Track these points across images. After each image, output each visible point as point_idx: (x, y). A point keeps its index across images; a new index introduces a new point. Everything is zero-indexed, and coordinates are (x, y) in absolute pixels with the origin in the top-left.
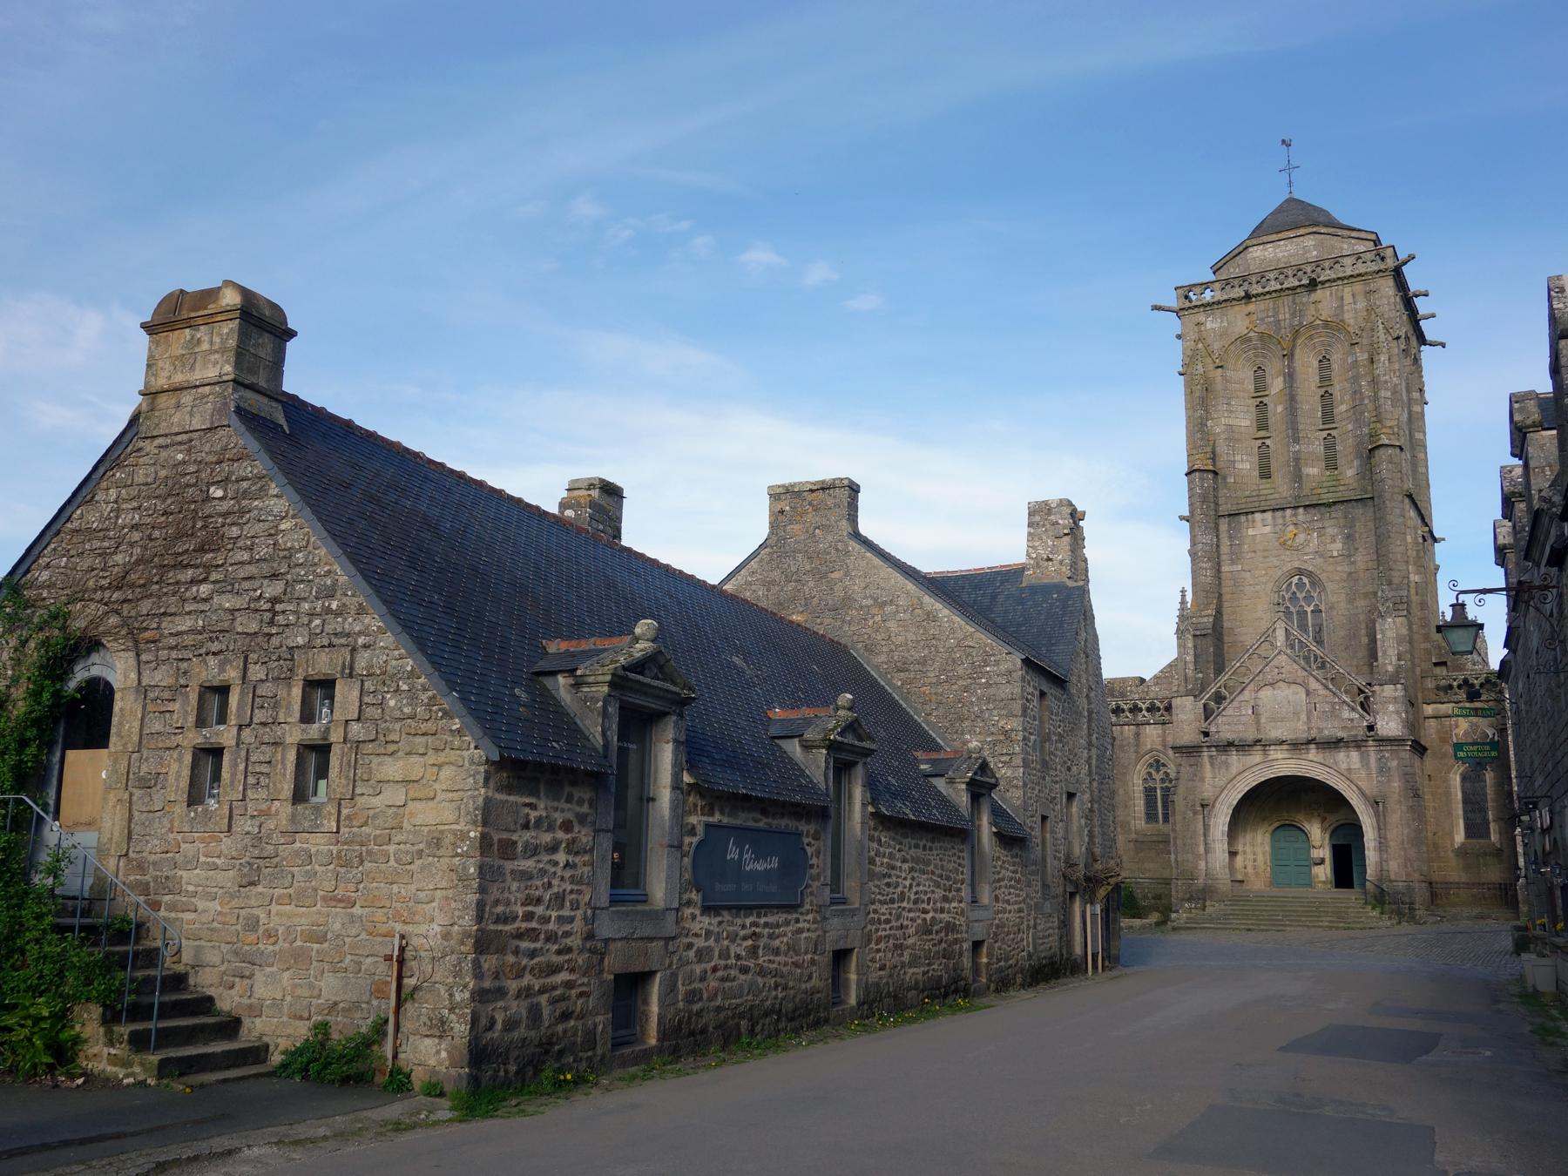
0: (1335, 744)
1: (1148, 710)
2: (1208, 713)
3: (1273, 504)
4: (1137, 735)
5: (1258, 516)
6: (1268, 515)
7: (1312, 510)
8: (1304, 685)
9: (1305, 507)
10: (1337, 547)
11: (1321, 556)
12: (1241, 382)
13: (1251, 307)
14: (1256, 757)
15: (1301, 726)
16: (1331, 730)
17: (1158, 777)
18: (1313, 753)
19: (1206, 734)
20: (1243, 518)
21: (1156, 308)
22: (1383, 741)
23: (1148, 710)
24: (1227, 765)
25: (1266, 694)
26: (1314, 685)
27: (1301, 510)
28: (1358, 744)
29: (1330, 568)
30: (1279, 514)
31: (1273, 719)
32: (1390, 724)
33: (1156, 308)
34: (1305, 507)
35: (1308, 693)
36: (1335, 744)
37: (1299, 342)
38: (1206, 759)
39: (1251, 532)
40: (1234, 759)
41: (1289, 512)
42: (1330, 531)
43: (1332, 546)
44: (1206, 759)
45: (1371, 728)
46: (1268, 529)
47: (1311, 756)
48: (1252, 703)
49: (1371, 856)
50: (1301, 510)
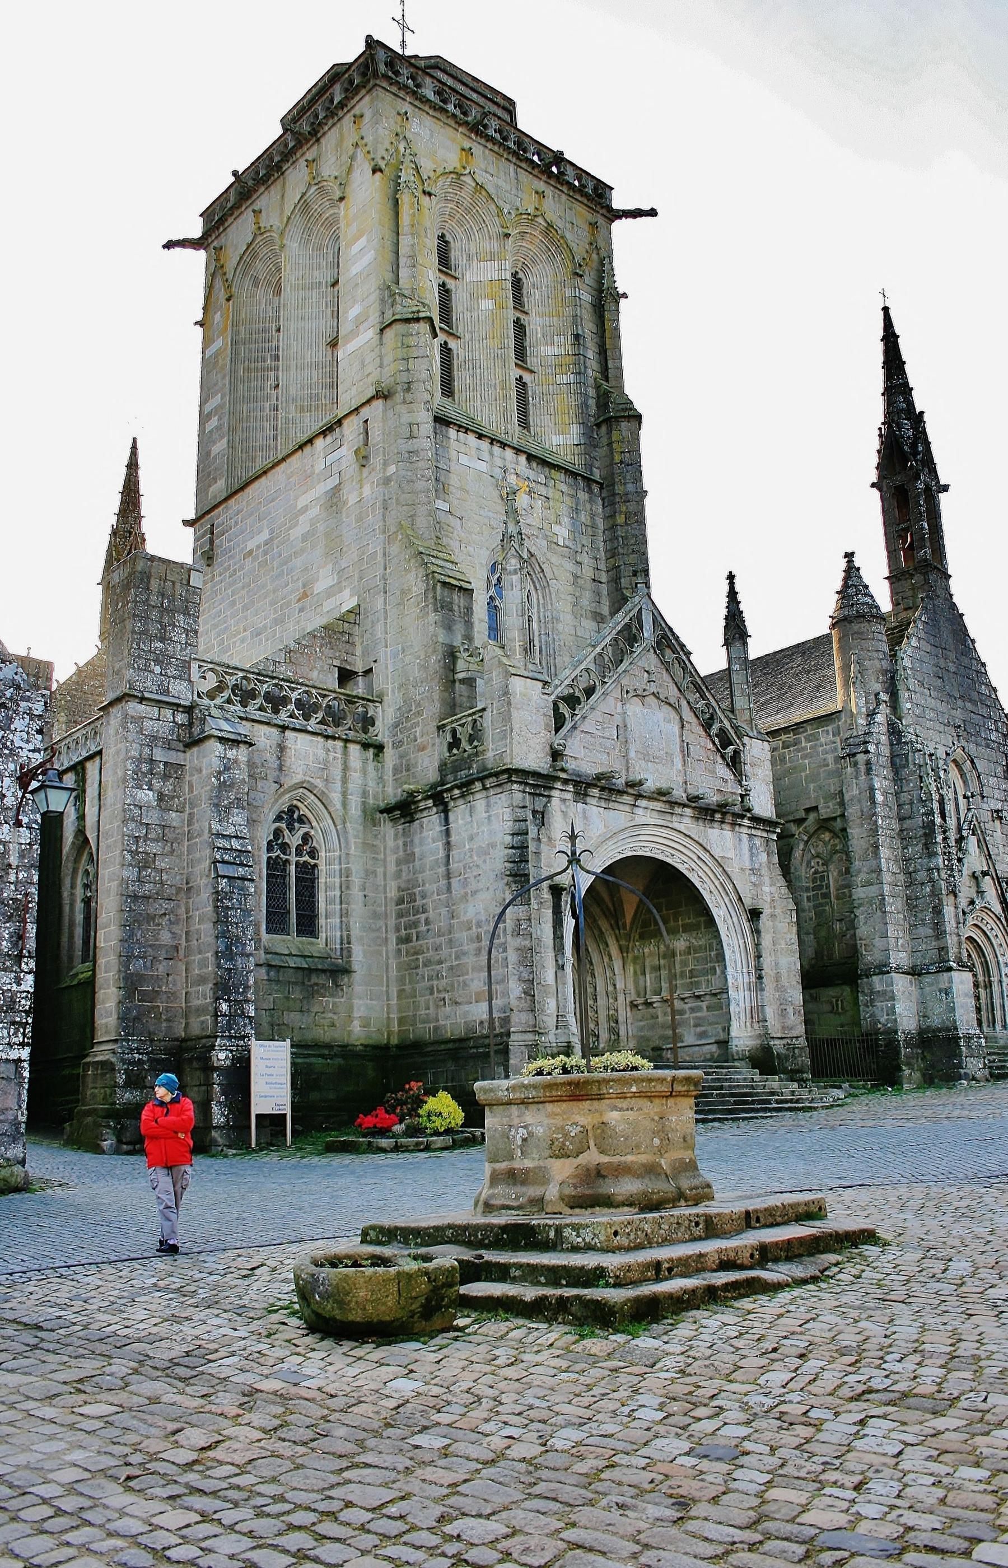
1: (299, 704)
4: (282, 748)
8: (677, 710)
17: (294, 840)
18: (686, 822)
22: (756, 820)
23: (299, 704)
25: (634, 708)
30: (497, 449)
31: (646, 757)
38: (555, 802)
43: (556, 528)
46: (482, 466)
47: (681, 827)
48: (618, 720)
49: (739, 999)
50: (523, 458)
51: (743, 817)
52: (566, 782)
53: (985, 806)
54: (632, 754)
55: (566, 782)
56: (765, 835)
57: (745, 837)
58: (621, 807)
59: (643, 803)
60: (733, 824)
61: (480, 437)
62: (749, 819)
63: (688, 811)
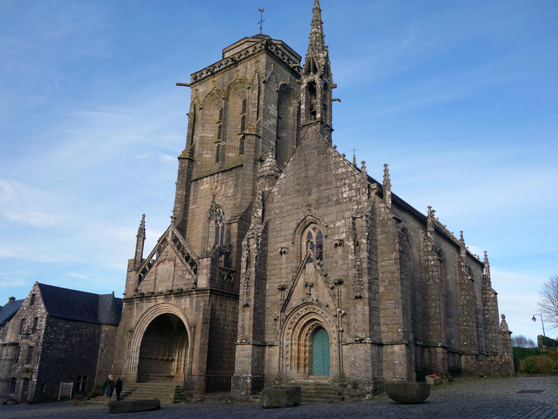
0: (180, 294)
2: (140, 279)
3: (211, 173)
5: (205, 179)
6: (209, 178)
7: (224, 174)
9: (222, 172)
10: (231, 191)
11: (225, 197)
12: (212, 116)
13: (215, 79)
14: (153, 304)
15: (170, 284)
16: (180, 284)
19: (137, 290)
20: (200, 181)
21: (178, 84)
24: (142, 307)
25: (161, 267)
26: (178, 261)
27: (220, 174)
28: (188, 293)
29: (227, 203)
30: (212, 177)
31: (161, 282)
32: (203, 282)
33: (178, 84)
34: (222, 172)
35: (175, 265)
36: (180, 294)
37: (231, 92)
38: (135, 305)
39: (202, 188)
40: (146, 305)
41: (216, 175)
42: (230, 183)
44: (135, 305)
45: (196, 283)
51: (192, 291)
52: (136, 298)
53: (328, 241)
54: (157, 282)
55: (136, 298)
56: (204, 295)
57: (195, 299)
58: (152, 301)
59: (158, 297)
60: (189, 295)
61: (207, 177)
62: (195, 291)
63: (172, 296)
